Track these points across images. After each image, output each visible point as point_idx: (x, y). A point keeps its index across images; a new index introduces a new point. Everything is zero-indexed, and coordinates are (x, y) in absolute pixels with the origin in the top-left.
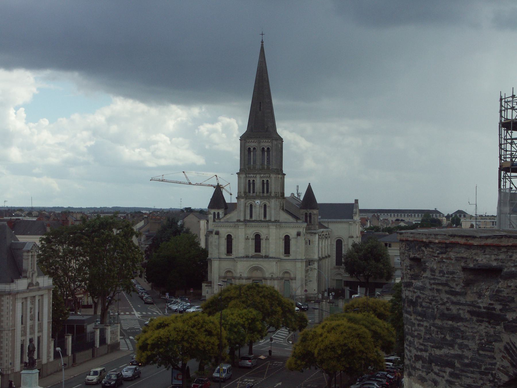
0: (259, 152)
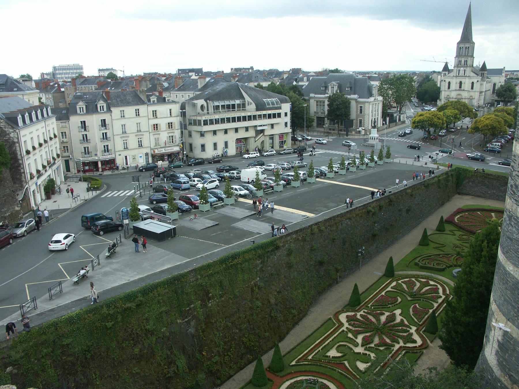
0: (464, 49)
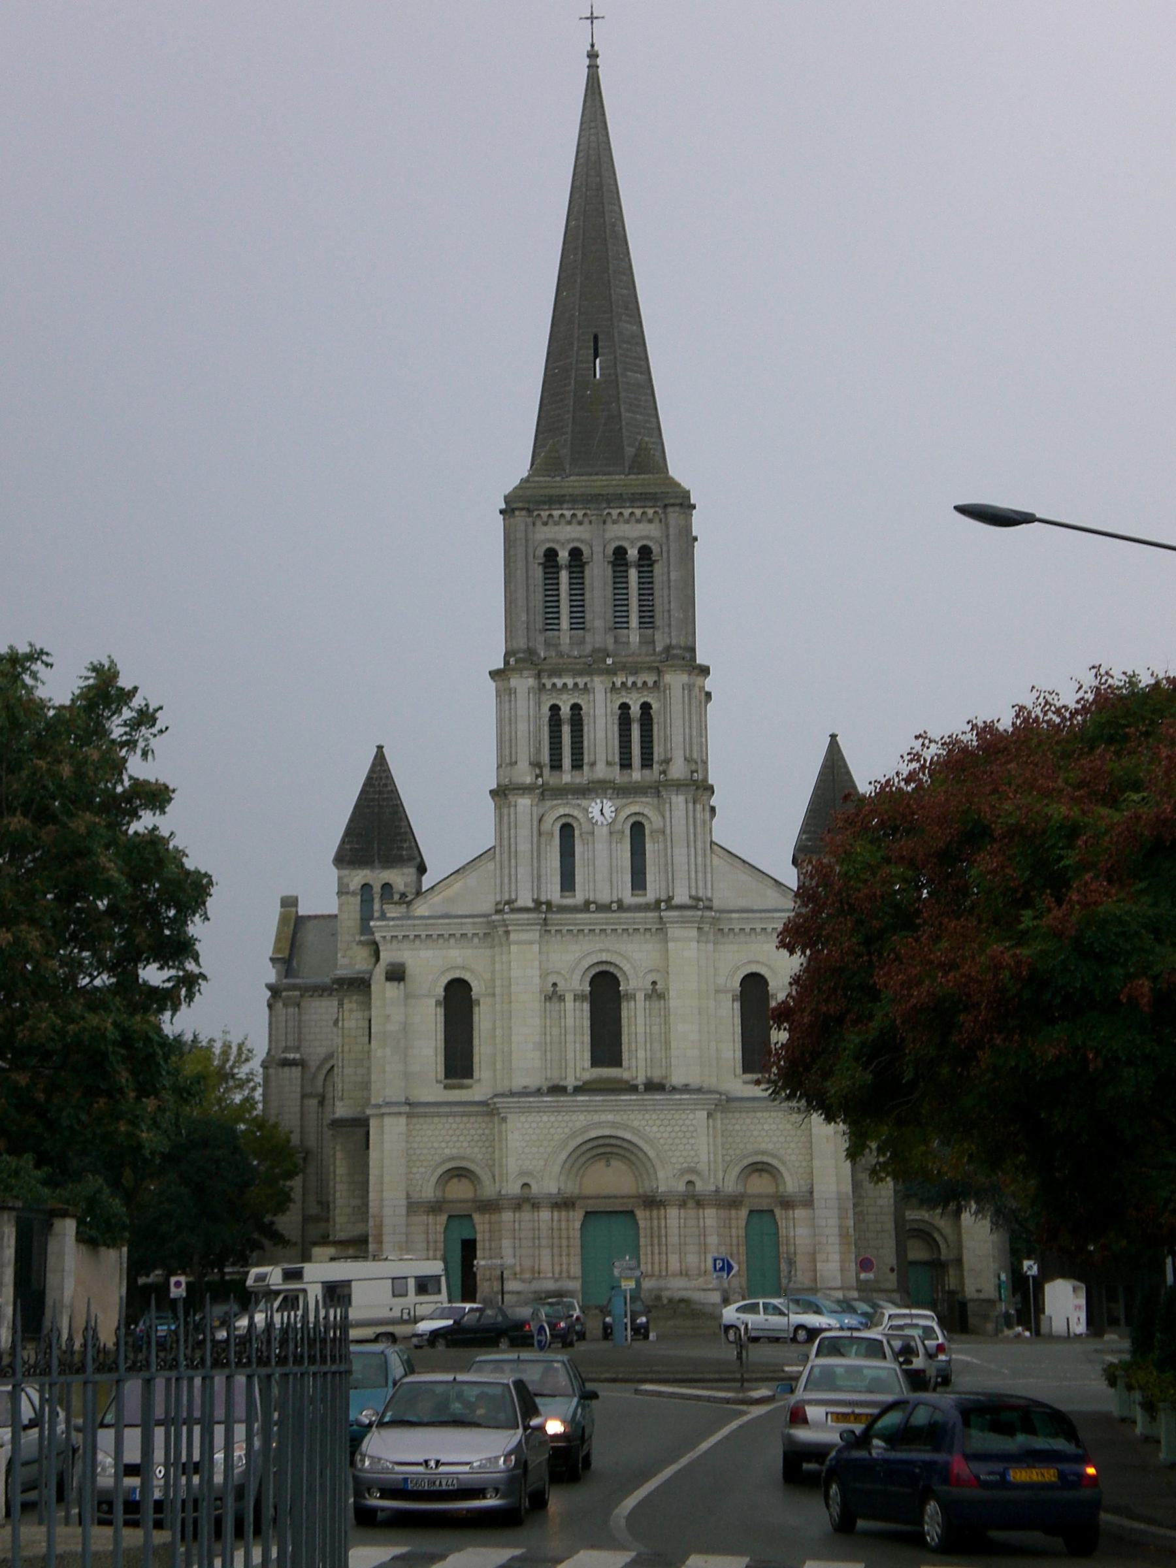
0: (598, 573)
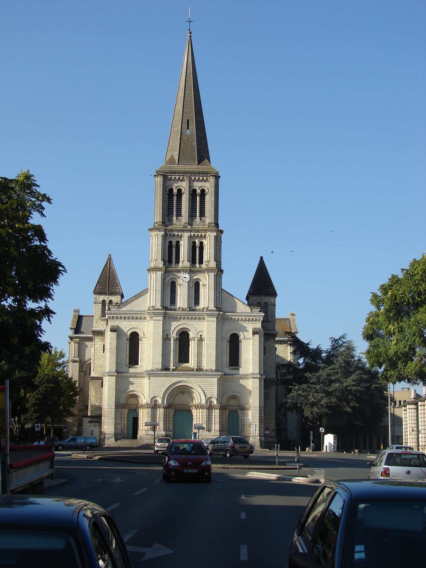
0: (185, 199)
